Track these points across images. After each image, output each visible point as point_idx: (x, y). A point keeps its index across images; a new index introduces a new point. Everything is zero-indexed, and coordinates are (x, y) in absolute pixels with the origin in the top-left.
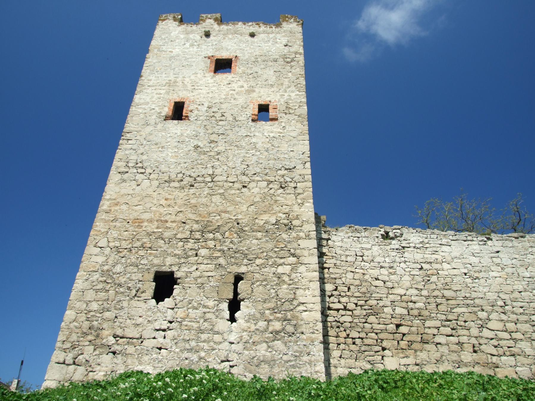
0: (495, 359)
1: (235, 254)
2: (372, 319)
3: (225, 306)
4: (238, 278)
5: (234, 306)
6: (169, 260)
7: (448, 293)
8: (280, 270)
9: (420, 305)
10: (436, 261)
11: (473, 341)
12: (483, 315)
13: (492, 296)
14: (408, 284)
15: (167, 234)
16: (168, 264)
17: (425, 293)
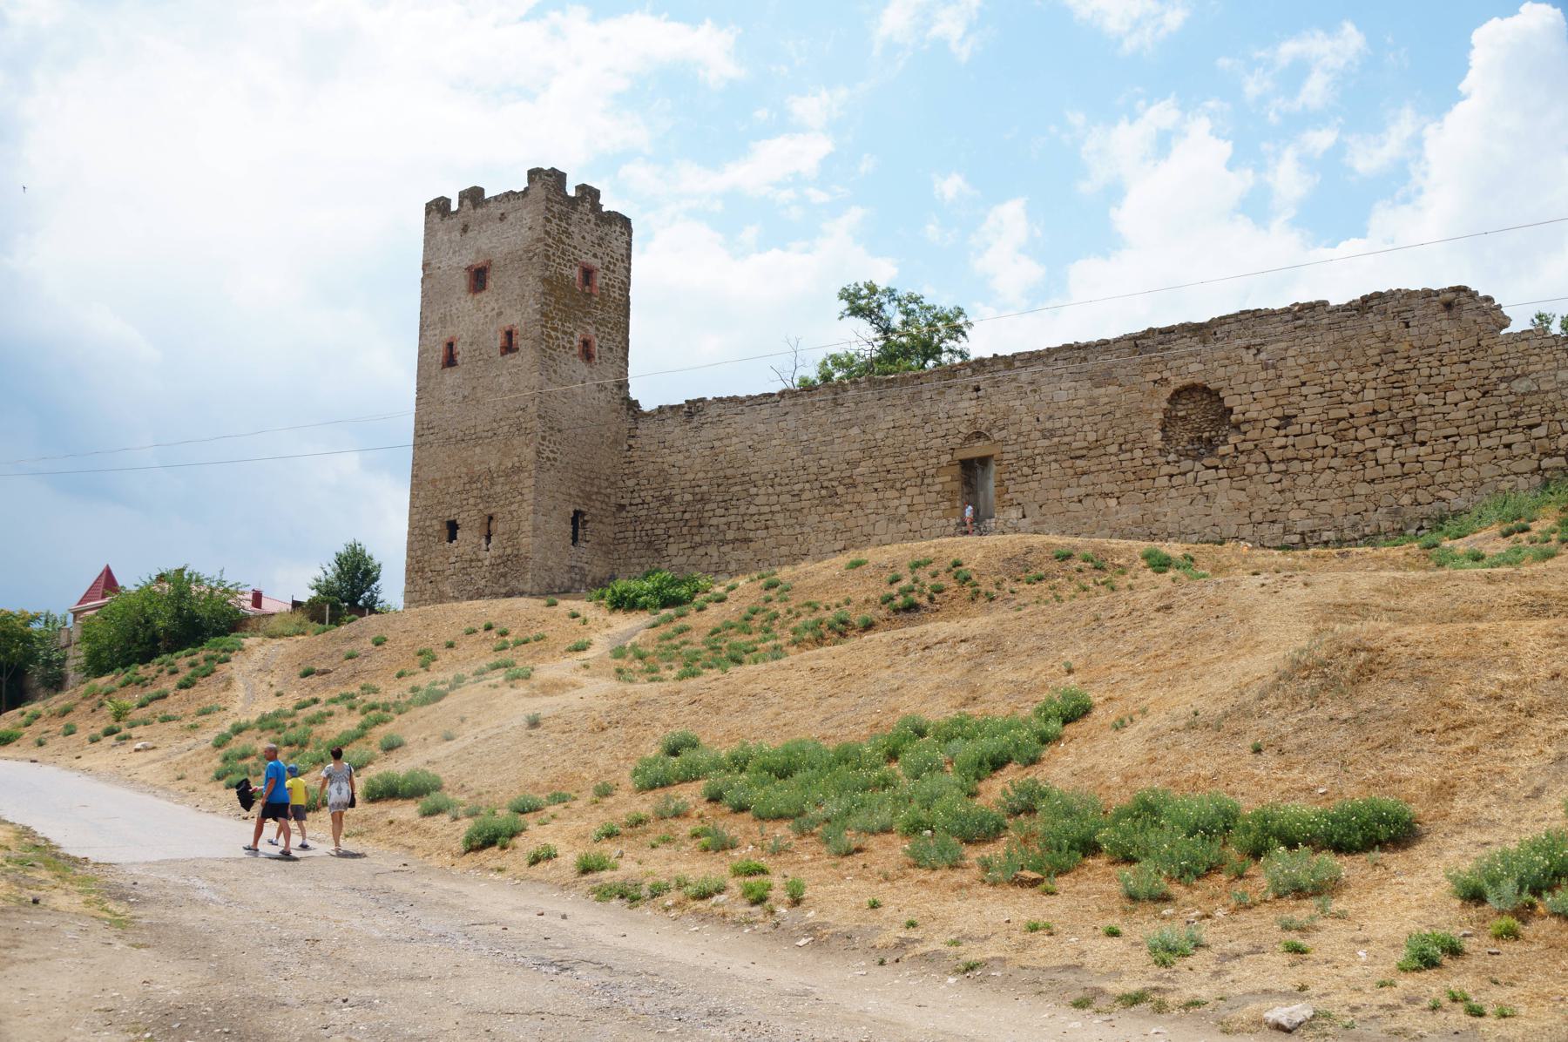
0: (751, 535)
1: (488, 499)
2: (664, 509)
3: (483, 541)
4: (491, 518)
5: (488, 538)
6: (454, 511)
7: (729, 472)
8: (513, 507)
9: (705, 488)
10: (729, 437)
11: (739, 519)
12: (753, 491)
13: (766, 468)
14: (698, 467)
15: (451, 490)
16: (452, 514)
17: (711, 475)
